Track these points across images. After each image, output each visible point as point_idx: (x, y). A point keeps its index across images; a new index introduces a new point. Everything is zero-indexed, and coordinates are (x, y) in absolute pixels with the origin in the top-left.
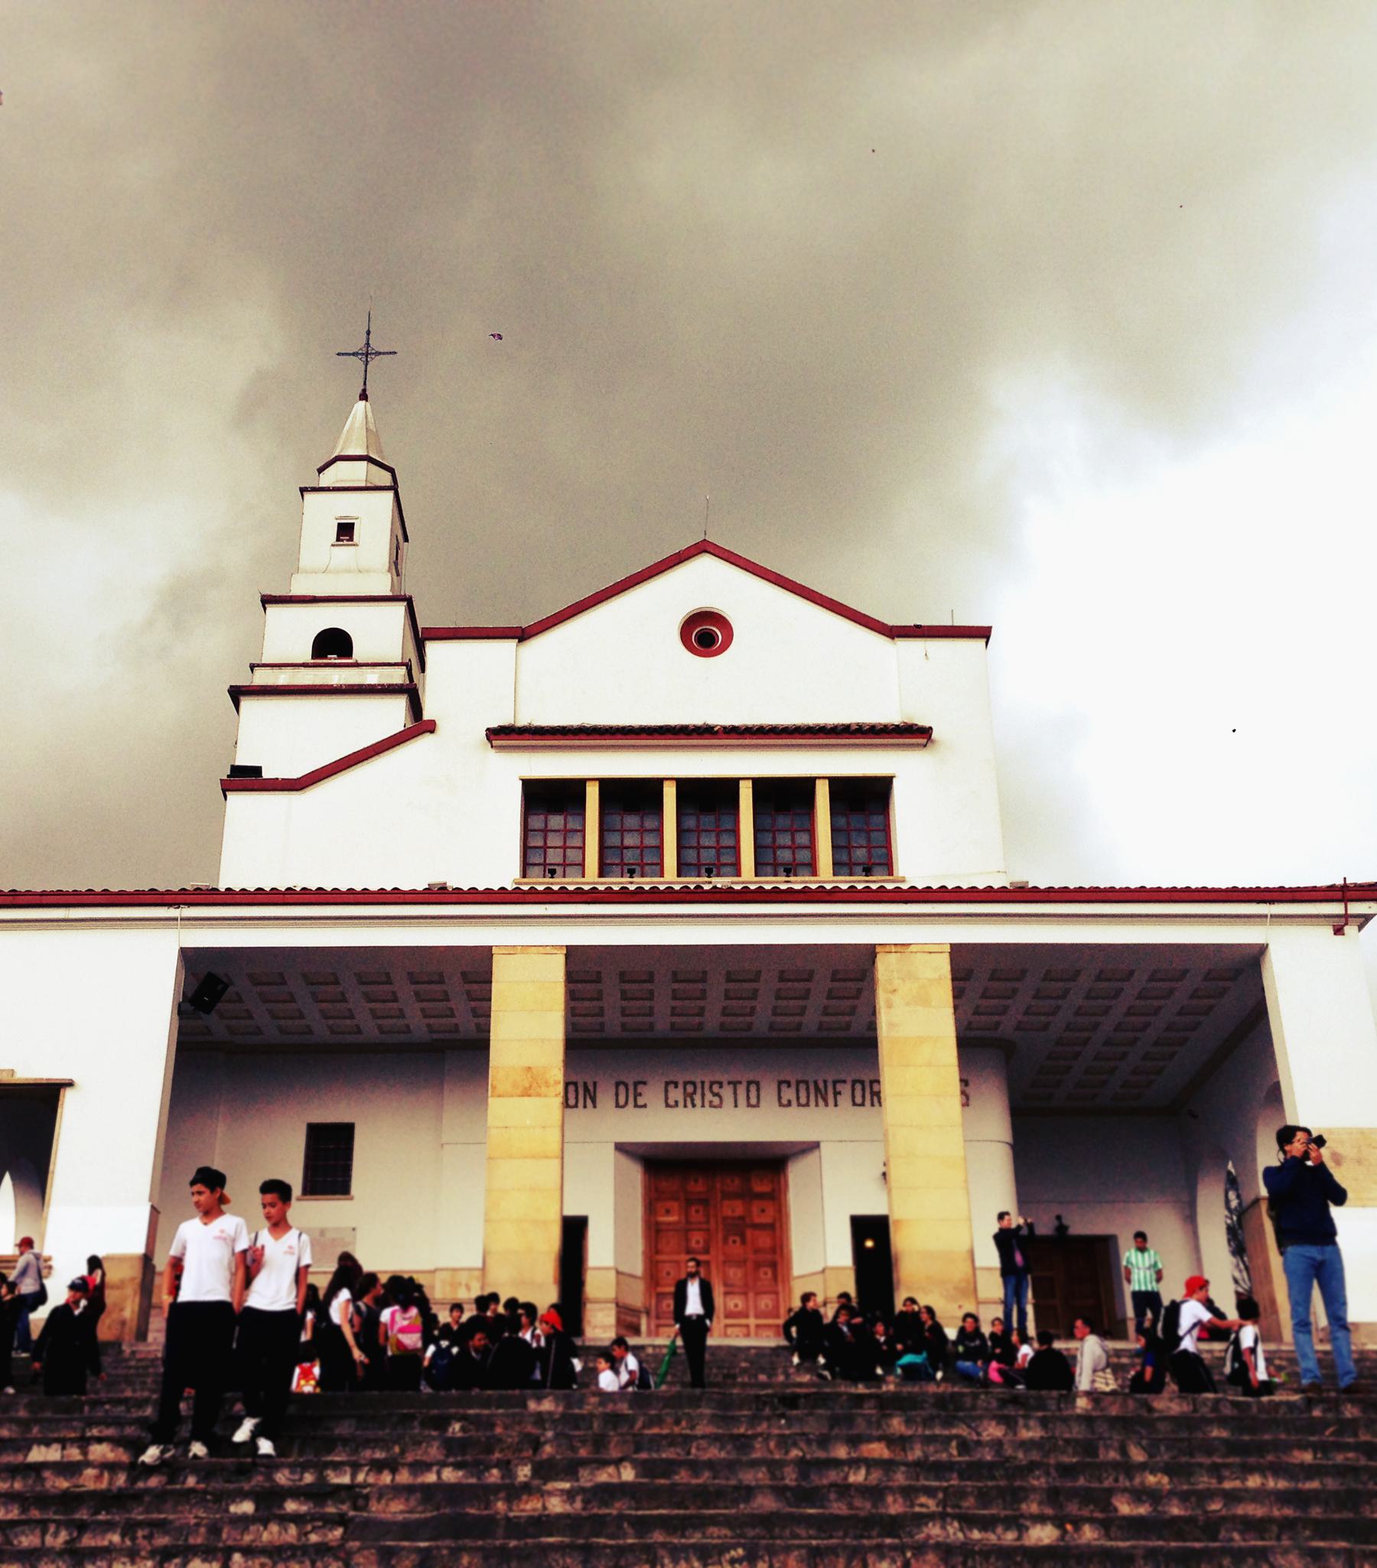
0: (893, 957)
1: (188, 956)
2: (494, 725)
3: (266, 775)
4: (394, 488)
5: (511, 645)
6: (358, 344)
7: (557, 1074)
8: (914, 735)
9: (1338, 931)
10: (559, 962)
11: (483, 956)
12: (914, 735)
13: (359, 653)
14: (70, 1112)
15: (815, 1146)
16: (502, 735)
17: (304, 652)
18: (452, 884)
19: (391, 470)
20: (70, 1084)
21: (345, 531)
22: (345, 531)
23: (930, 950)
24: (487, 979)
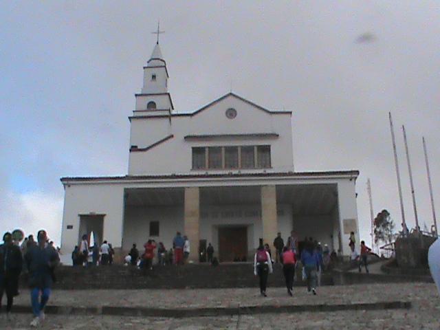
0: (264, 187)
1: (126, 190)
2: (186, 135)
3: (139, 147)
4: (165, 67)
5: (189, 118)
6: (156, 31)
7: (198, 212)
8: (275, 136)
9: (351, 180)
10: (198, 191)
11: (183, 188)
12: (275, 136)
13: (158, 108)
14: (106, 219)
15: (253, 224)
16: (188, 138)
17: (145, 107)
18: (176, 174)
19: (164, 61)
20: (104, 215)
21: (154, 77)
22: (154, 77)
23: (272, 186)
24: (184, 191)
